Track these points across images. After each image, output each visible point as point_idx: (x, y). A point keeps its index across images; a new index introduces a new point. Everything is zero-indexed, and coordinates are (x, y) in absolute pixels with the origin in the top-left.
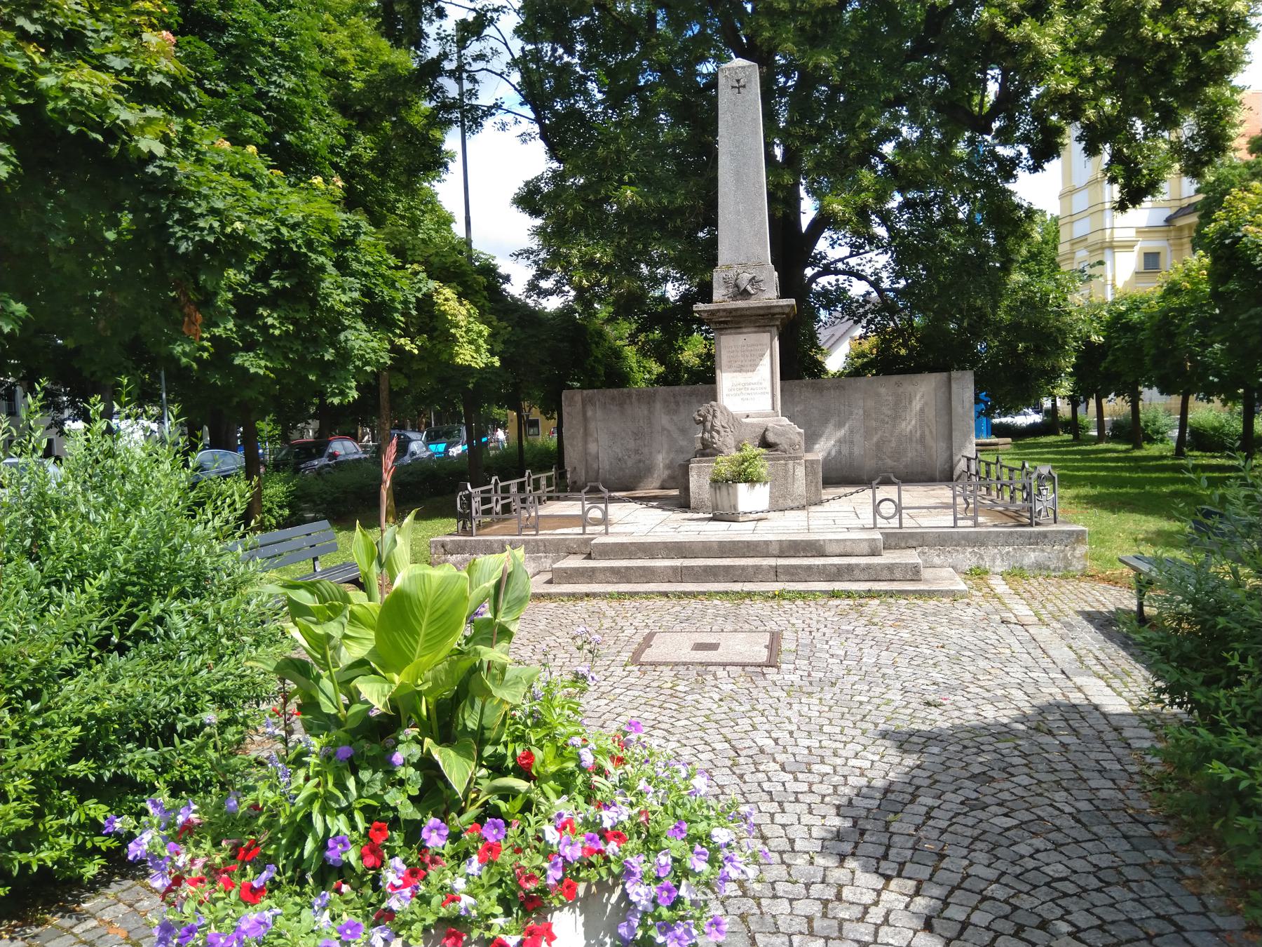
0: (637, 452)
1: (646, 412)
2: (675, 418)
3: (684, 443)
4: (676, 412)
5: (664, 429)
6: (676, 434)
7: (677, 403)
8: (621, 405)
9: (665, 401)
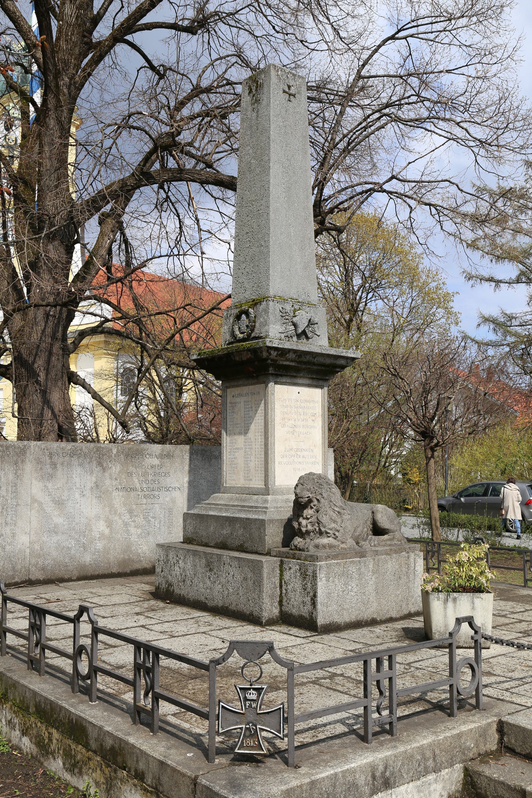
1: (11, 477)
2: (50, 485)
3: (59, 520)
4: (51, 477)
5: (34, 500)
6: (49, 507)
7: (54, 465)
9: (39, 461)
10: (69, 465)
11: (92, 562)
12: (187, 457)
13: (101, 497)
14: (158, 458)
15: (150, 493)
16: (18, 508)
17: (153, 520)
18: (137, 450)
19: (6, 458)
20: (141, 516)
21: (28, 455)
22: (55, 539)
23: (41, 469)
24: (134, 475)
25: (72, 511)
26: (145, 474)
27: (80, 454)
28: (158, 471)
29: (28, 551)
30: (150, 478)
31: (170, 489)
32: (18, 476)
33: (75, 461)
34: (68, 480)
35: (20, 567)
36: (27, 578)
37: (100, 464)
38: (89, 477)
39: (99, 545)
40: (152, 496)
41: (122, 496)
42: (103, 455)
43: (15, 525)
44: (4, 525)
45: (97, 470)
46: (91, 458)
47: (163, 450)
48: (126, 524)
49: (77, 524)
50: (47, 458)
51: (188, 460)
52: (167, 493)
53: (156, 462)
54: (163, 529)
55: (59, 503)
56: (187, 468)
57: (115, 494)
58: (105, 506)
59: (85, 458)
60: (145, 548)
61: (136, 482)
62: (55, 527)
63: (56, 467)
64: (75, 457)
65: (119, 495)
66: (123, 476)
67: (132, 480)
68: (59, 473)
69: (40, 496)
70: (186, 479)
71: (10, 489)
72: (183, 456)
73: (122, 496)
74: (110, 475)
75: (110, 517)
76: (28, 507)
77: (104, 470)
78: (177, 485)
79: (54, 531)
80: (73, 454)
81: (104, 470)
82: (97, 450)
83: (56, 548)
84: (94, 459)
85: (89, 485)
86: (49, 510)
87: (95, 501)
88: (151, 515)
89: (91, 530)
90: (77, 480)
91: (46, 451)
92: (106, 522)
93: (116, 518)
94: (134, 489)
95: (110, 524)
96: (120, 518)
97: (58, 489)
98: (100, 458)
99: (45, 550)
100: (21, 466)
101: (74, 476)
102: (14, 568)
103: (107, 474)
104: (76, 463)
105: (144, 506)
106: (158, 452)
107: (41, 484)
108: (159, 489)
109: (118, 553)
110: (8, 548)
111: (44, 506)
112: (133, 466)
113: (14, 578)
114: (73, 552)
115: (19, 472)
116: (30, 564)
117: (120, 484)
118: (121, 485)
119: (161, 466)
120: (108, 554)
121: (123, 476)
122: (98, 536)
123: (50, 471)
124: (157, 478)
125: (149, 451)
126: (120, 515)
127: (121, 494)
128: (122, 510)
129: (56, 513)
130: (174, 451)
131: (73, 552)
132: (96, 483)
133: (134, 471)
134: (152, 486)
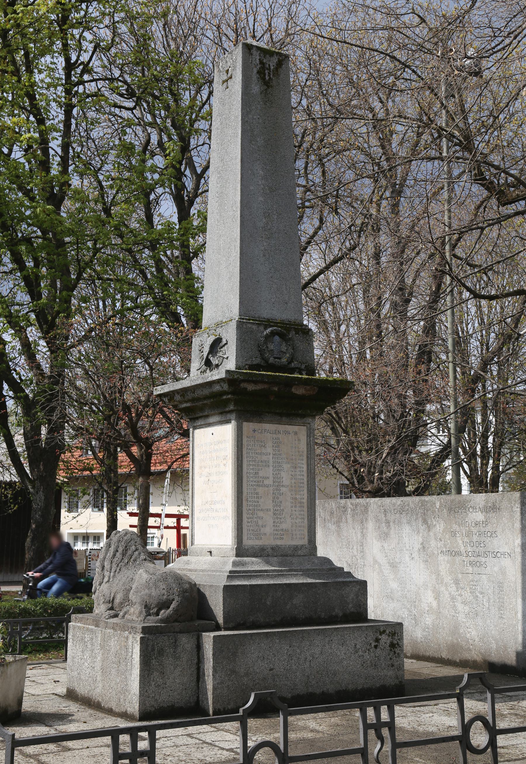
2: (386, 545)
5: (375, 561)
6: (387, 570)
9: (378, 520)
10: (400, 523)
11: (423, 640)
12: (517, 508)
13: (427, 561)
15: (476, 559)
21: (369, 513)
23: (379, 527)
27: (408, 510)
28: (483, 530)
30: (475, 538)
37: (425, 521)
38: (416, 538)
39: (428, 620)
45: (422, 528)
46: (417, 515)
48: (453, 598)
49: (408, 591)
50: (383, 516)
51: (519, 514)
52: (495, 560)
53: (480, 516)
55: (394, 566)
56: (518, 525)
57: (441, 558)
60: (474, 633)
63: (389, 526)
68: (392, 532)
70: (518, 541)
77: (429, 528)
78: (506, 549)
80: (402, 511)
81: (429, 528)
82: (422, 505)
84: (419, 515)
85: (417, 546)
87: (422, 566)
92: (433, 592)
95: (437, 596)
103: (431, 534)
105: (470, 575)
106: (482, 504)
108: (486, 554)
109: (446, 634)
112: (456, 523)
117: (445, 546)
118: (446, 548)
119: (486, 523)
121: (447, 536)
122: (427, 609)
125: (472, 504)
127: (446, 558)
128: (448, 579)
132: (422, 544)
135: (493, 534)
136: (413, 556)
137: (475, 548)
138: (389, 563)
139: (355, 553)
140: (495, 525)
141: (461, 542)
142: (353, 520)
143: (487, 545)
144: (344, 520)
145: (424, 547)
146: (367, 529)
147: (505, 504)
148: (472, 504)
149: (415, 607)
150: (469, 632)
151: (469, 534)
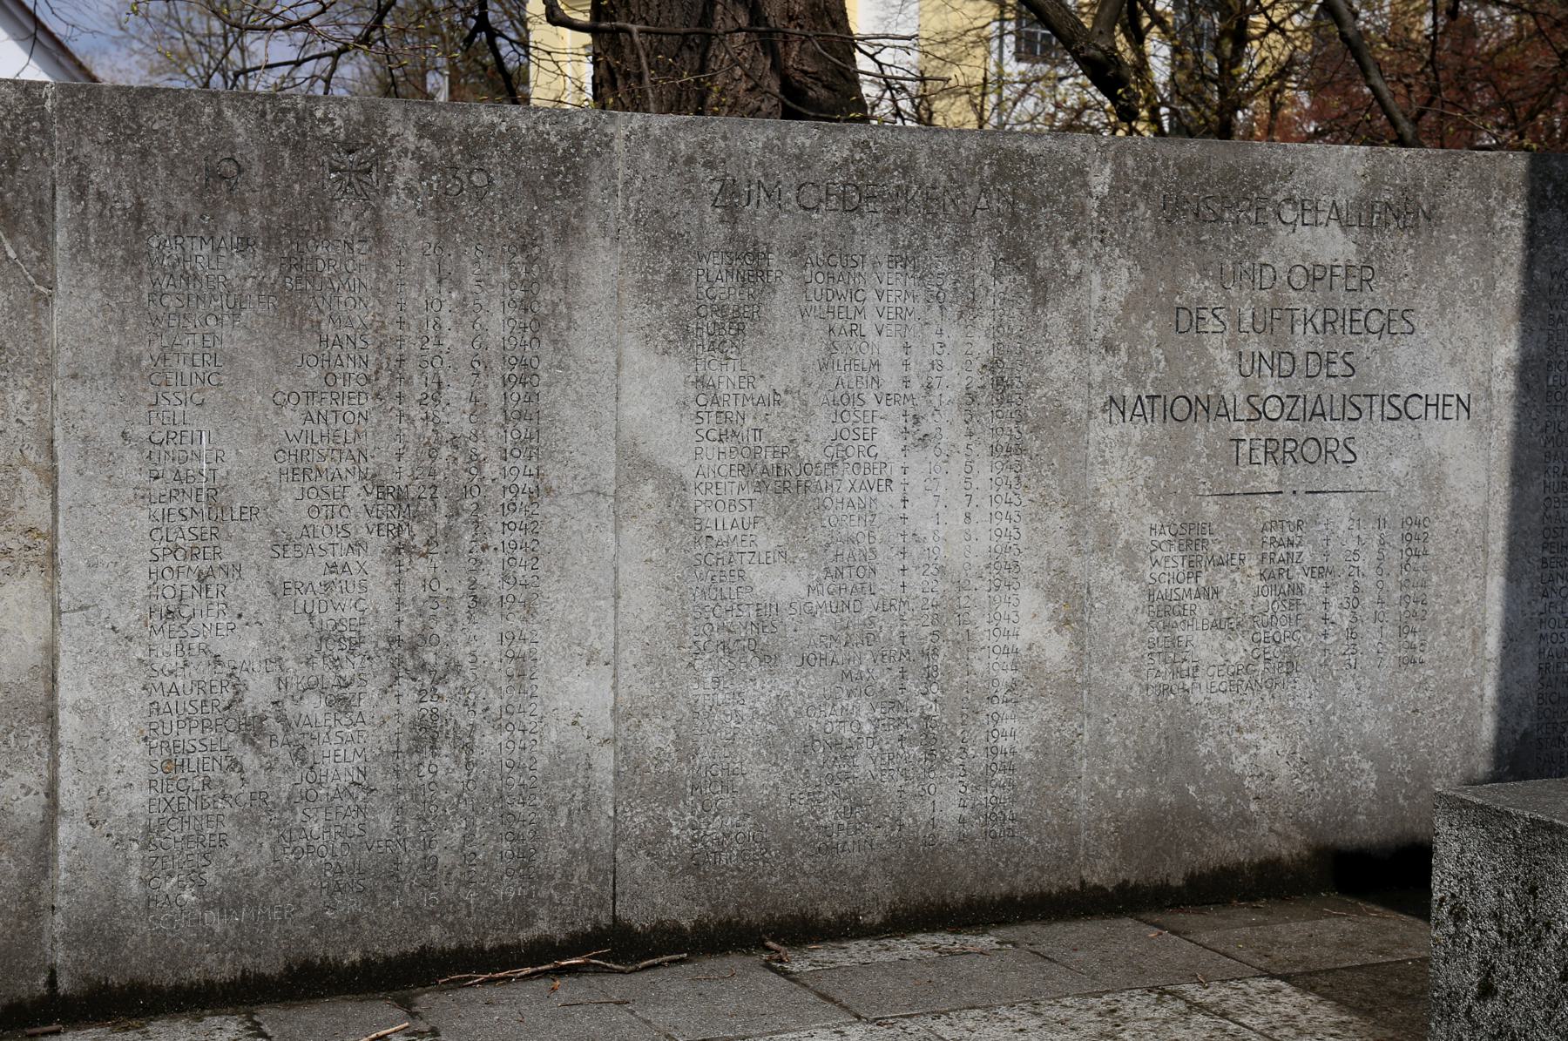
0: (408, 655)
1: (498, 323)
2: (726, 376)
3: (782, 584)
4: (734, 326)
5: (638, 464)
6: (728, 508)
7: (750, 260)
8: (291, 240)
9: (659, 233)
10: (842, 259)
11: (974, 829)
12: (1512, 220)
13: (1021, 450)
14: (1345, 227)
15: (1301, 430)
16: (546, 507)
17: (1317, 586)
18: (1230, 175)
19: (466, 208)
20: (1252, 562)
21: (595, 193)
22: (762, 691)
23: (675, 278)
24: (1212, 325)
25: (857, 528)
26: (1274, 319)
27: (902, 191)
28: (1345, 302)
29: (605, 761)
30: (1302, 340)
31: (1416, 407)
32: (539, 321)
33: (872, 238)
34: (832, 347)
35: (560, 854)
36: (605, 919)
37: (1016, 256)
38: (953, 334)
39: (1016, 730)
40: (1311, 450)
41: (1144, 448)
42: (1033, 203)
43: (528, 606)
44: (462, 607)
45: (998, 290)
46: (966, 221)
47: (1375, 180)
48: (1165, 611)
49: (886, 606)
50: (712, 216)
51: (1518, 241)
53: (1334, 245)
54: (1371, 636)
55: (784, 483)
56: (1510, 286)
57: (1103, 430)
58: (1045, 502)
59: (931, 219)
60: (1270, 746)
61: (1222, 363)
62: (760, 625)
63: (760, 272)
64: (875, 213)
65: (1123, 441)
66: (1149, 331)
67: (1202, 351)
68: (781, 304)
69: (672, 439)
70: (1507, 351)
71: (494, 393)
72: (1490, 213)
73: (1144, 448)
74: (1077, 321)
75: (1076, 566)
76: (604, 505)
78: (1453, 384)
79: (756, 644)
81: (1041, 290)
82: (1001, 174)
83: (769, 743)
84: (981, 223)
85: (955, 379)
86: (720, 521)
87: (985, 472)
88: (1307, 554)
89: (965, 643)
90: (887, 347)
91: (700, 172)
92: (1051, 593)
93: (1110, 573)
94: (1210, 407)
95: (1072, 607)
96: (1131, 574)
97: (776, 398)
98: (1014, 219)
99: (705, 757)
100: (556, 262)
101: (868, 327)
102: (525, 859)
103: (1055, 318)
104: (878, 248)
106: (1350, 190)
107: (672, 372)
109: (1120, 775)
110: (490, 742)
111: (694, 498)
112: (1203, 271)
113: (528, 919)
114: (864, 766)
115: (547, 295)
116: (618, 838)
117: (1133, 374)
118: (1138, 382)
119: (1364, 272)
120: (1063, 779)
121: (1149, 331)
122: (1006, 677)
123: (726, 290)
124: (1343, 341)
125: (1297, 185)
126: (1130, 555)
127: (1137, 431)
128: (1140, 524)
129: (765, 542)
130: (1438, 187)
131: (864, 766)
132: (992, 365)
133: (1214, 297)
134: (1312, 391)
135: (1397, 321)
136: (927, 426)
137: (1298, 381)
138: (746, 469)
139: (458, 421)
140: (1405, 285)
141: (1227, 355)
142: (443, 232)
143: (1362, 369)
144: (346, 218)
145: (999, 383)
146: (569, 281)
147: (1459, 193)
148: (1297, 185)
149: (929, 678)
150: (1245, 749)
151: (1274, 319)
